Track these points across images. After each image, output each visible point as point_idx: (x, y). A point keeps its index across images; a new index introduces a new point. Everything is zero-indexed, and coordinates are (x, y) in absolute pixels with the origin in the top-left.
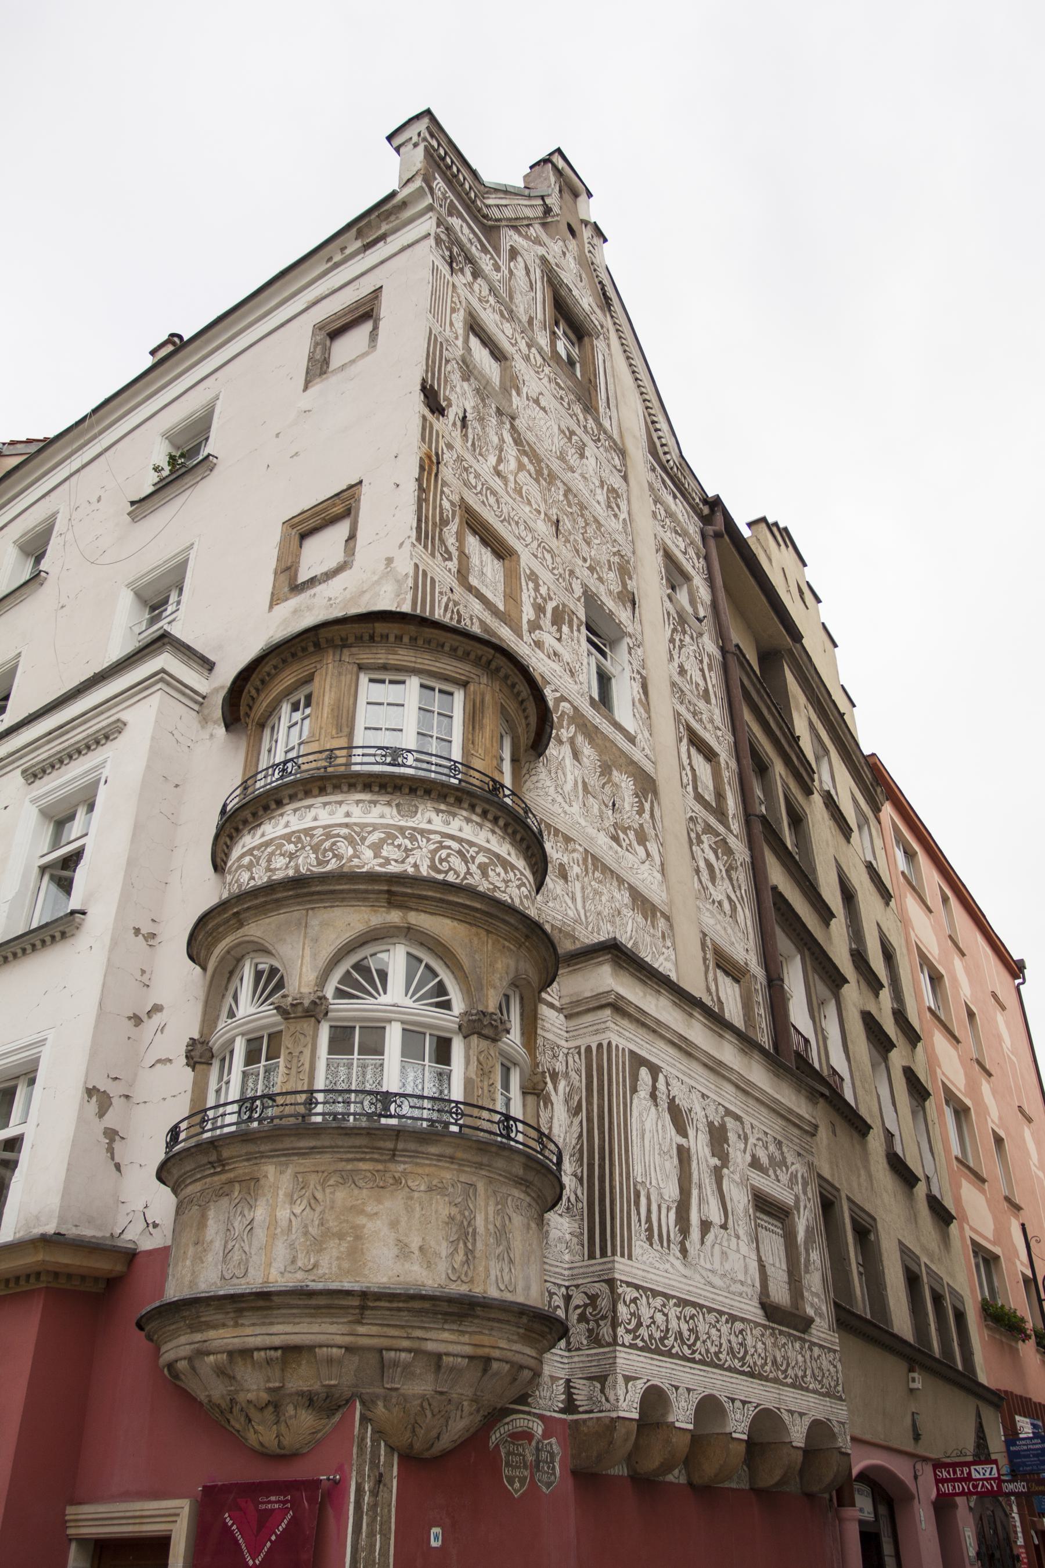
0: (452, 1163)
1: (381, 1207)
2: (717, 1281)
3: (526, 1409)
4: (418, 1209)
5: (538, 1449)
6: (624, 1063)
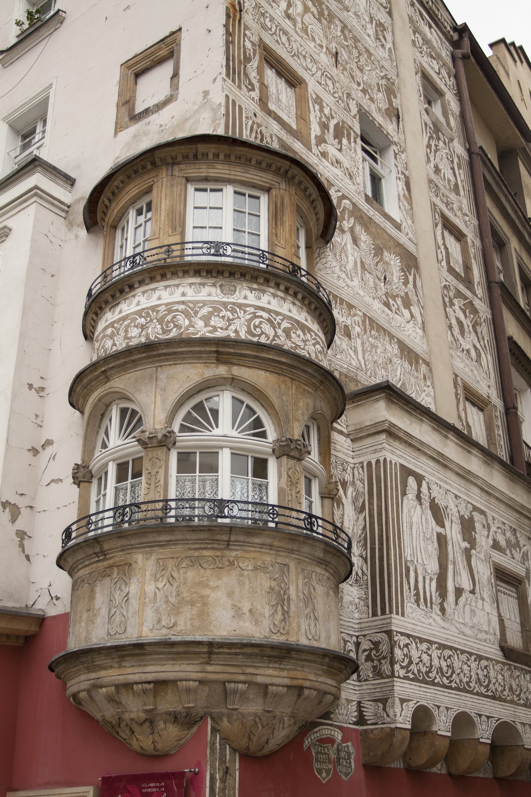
0: (271, 549)
1: (221, 582)
3: (330, 722)
4: (247, 583)
5: (338, 750)
6: (396, 474)
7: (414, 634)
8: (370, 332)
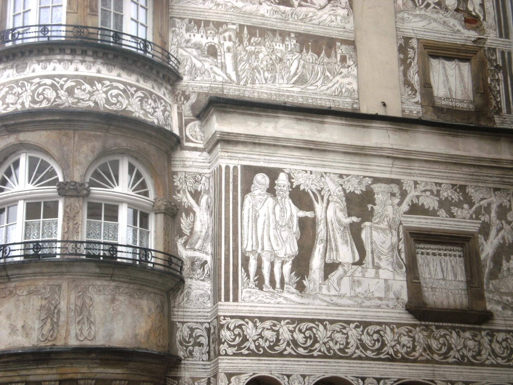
0: (44, 276)
4: (22, 306)
7: (252, 315)
8: (249, 40)
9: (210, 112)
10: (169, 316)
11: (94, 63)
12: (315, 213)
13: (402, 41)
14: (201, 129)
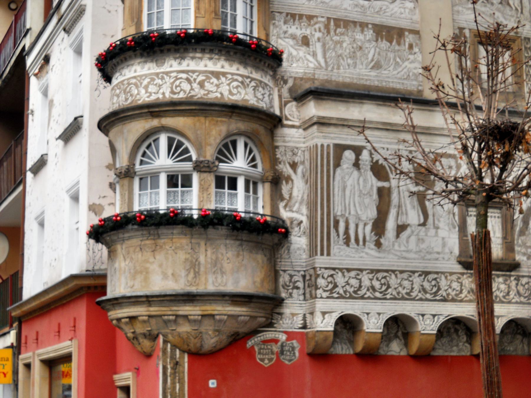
2: (412, 255)
5: (282, 346)
6: (328, 154)
7: (341, 267)
9: (307, 97)
10: (275, 265)
11: (219, 59)
12: (390, 183)
13: (457, 32)
14: (297, 109)
